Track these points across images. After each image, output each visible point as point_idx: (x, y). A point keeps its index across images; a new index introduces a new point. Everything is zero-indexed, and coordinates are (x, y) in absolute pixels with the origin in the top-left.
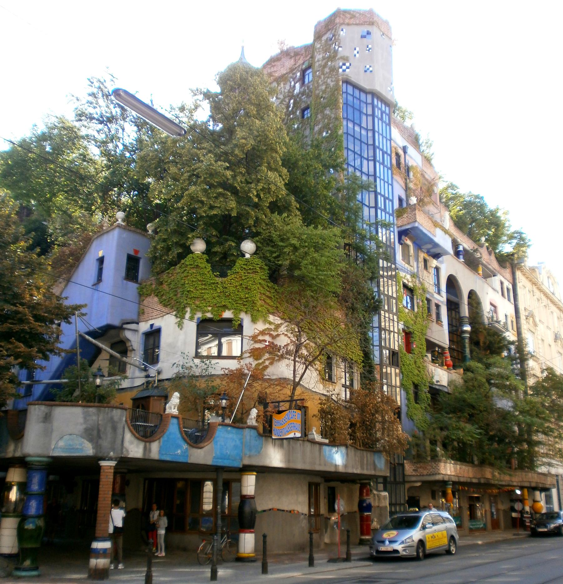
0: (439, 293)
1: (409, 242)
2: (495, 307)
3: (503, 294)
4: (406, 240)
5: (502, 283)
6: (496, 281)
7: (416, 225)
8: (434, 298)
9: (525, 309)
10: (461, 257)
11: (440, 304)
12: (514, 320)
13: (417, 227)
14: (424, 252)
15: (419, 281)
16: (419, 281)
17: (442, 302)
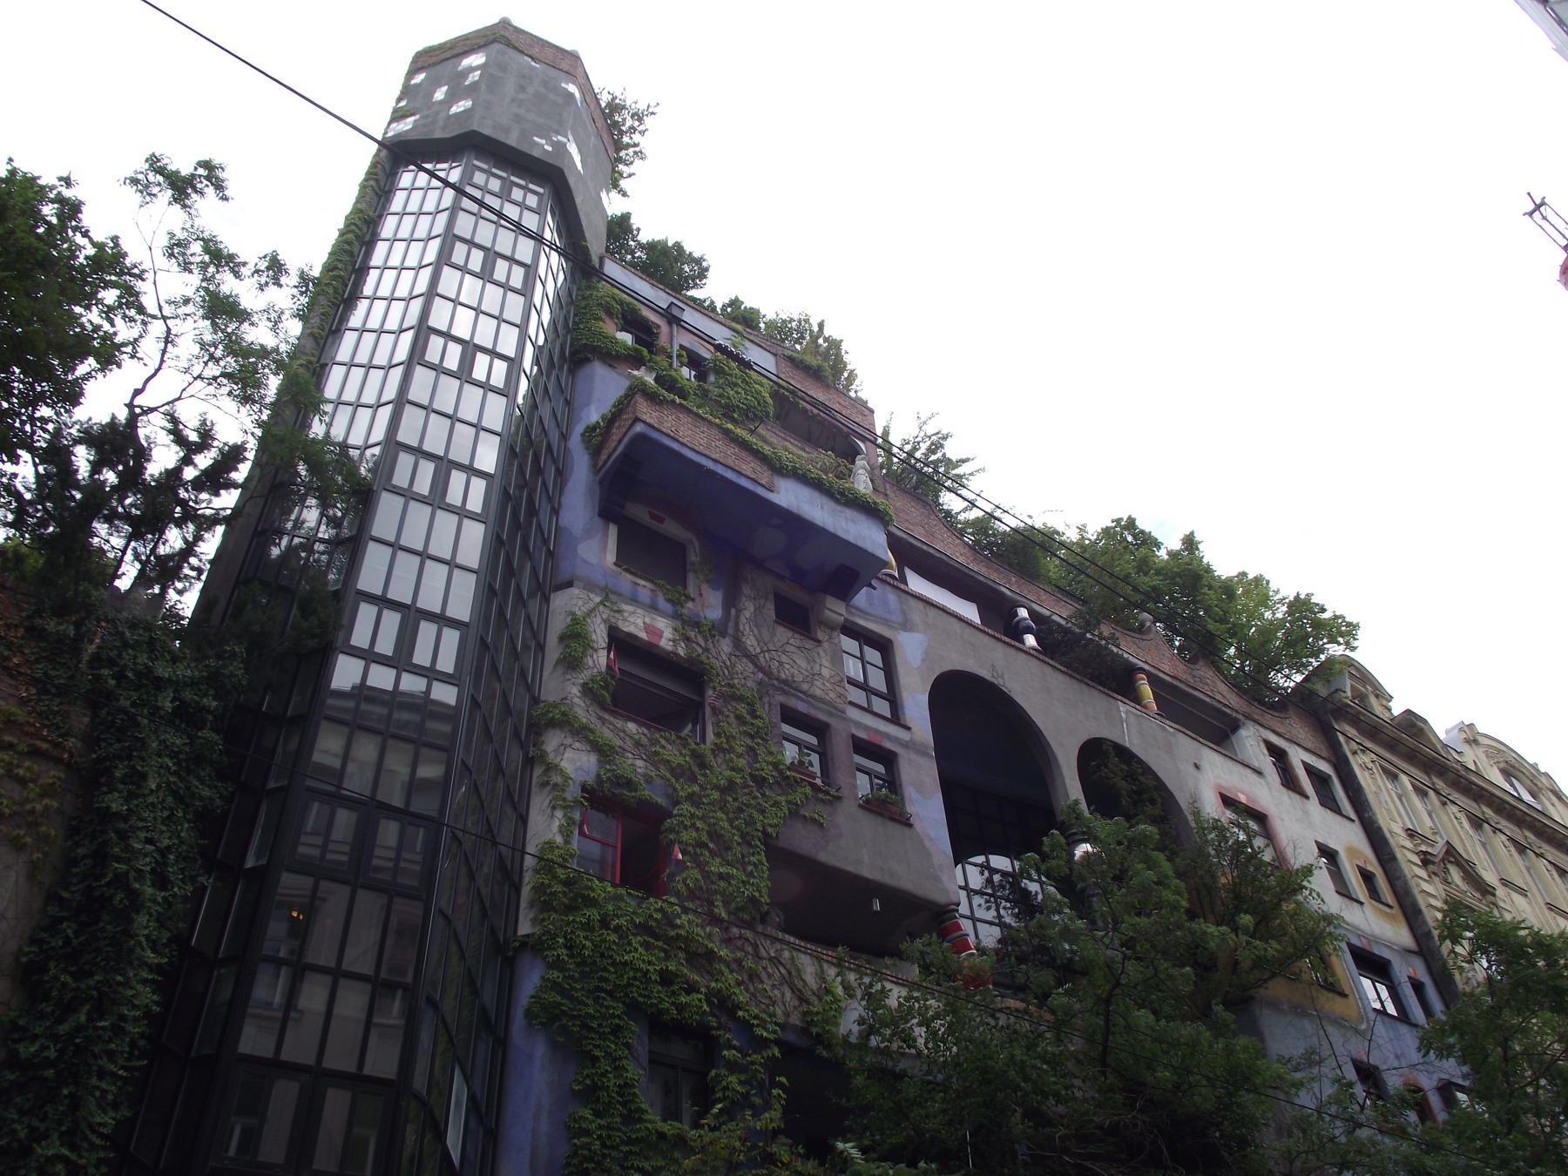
0: (896, 718)
1: (671, 528)
2: (1261, 818)
3: (1289, 781)
4: (661, 520)
5: (1278, 755)
6: (1250, 740)
7: (639, 428)
8: (846, 719)
9: (1411, 834)
10: (1030, 640)
11: (888, 745)
12: (1374, 867)
13: (641, 438)
14: (781, 577)
15: (738, 644)
16: (738, 644)
17: (906, 745)
